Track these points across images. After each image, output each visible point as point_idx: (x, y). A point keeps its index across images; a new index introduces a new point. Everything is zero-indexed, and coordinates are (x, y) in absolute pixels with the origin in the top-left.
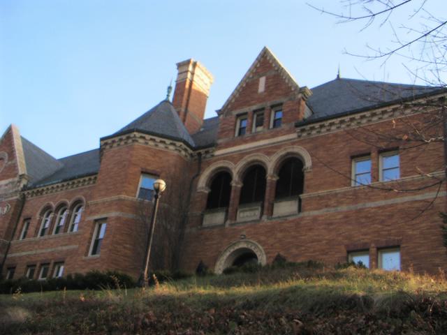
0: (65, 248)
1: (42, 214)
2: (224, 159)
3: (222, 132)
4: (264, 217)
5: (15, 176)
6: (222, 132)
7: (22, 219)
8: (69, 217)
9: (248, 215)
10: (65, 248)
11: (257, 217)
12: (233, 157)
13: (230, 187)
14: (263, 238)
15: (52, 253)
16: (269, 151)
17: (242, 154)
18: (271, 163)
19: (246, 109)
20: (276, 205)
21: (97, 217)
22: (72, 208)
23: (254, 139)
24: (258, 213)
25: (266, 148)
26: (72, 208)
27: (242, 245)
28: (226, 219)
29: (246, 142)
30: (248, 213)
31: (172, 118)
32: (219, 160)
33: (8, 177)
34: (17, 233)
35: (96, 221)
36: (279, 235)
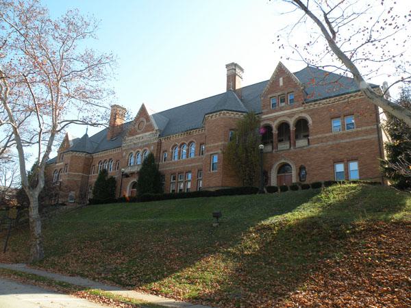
0: (190, 165)
1: (172, 149)
2: (268, 119)
3: (264, 106)
4: (292, 148)
5: (153, 130)
6: (264, 106)
7: (162, 152)
8: (188, 150)
9: (284, 146)
10: (190, 165)
11: (288, 148)
12: (273, 118)
13: (272, 134)
14: (293, 157)
15: (184, 168)
16: (290, 116)
17: (276, 118)
18: (292, 122)
19: (274, 95)
20: (297, 142)
21: (212, 153)
22: (180, 147)
23: (281, 109)
24: (288, 145)
25: (288, 114)
26: (180, 147)
27: (283, 161)
28: (273, 149)
29: (277, 111)
30: (283, 146)
31: (233, 96)
32: (265, 120)
33: (149, 131)
34: (161, 159)
35: (211, 155)
36: (300, 156)
